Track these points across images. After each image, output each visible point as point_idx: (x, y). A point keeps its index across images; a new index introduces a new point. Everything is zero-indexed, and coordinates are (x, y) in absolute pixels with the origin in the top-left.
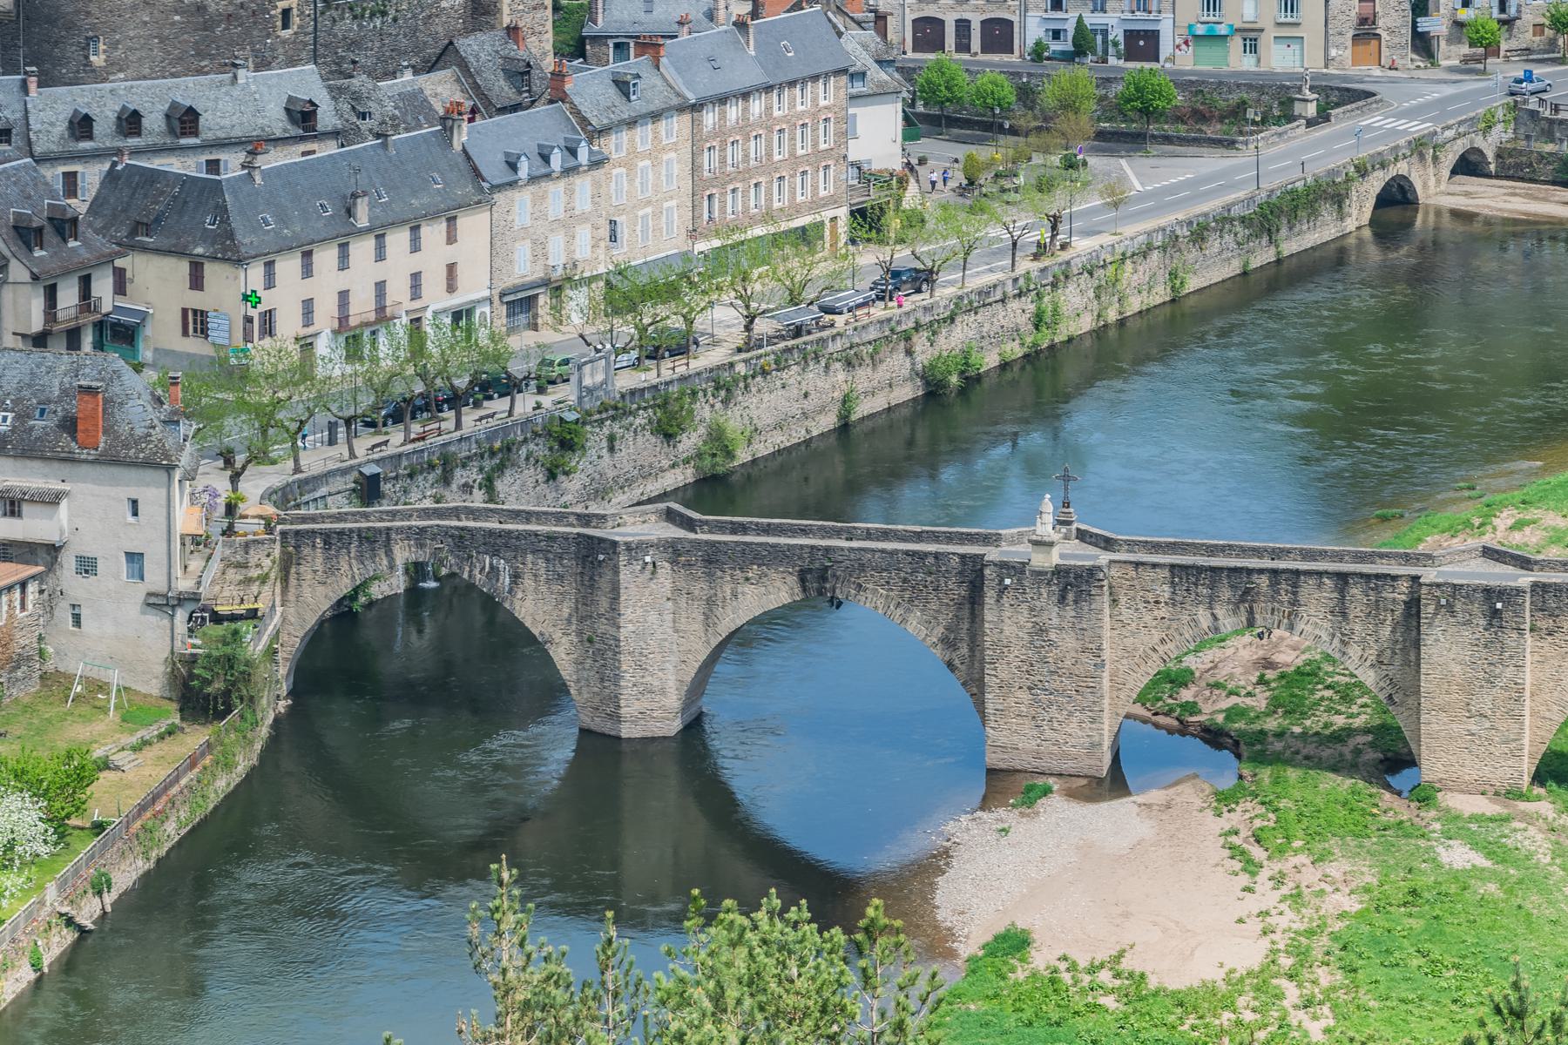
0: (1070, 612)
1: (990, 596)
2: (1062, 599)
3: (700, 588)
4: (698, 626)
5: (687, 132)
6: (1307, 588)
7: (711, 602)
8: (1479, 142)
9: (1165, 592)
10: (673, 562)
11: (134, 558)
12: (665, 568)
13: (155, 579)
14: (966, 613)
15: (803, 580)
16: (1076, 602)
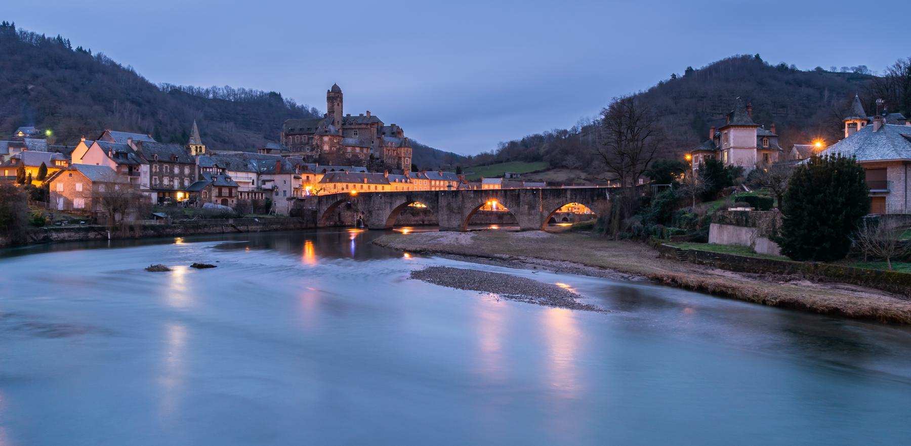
0: (454, 200)
1: (440, 198)
2: (453, 197)
3: (389, 201)
4: (389, 208)
5: (429, 184)
6: (499, 193)
7: (391, 203)
8: (567, 217)
9: (472, 196)
10: (385, 196)
11: (285, 191)
12: (383, 198)
13: (288, 195)
14: (436, 202)
15: (407, 198)
16: (456, 197)
